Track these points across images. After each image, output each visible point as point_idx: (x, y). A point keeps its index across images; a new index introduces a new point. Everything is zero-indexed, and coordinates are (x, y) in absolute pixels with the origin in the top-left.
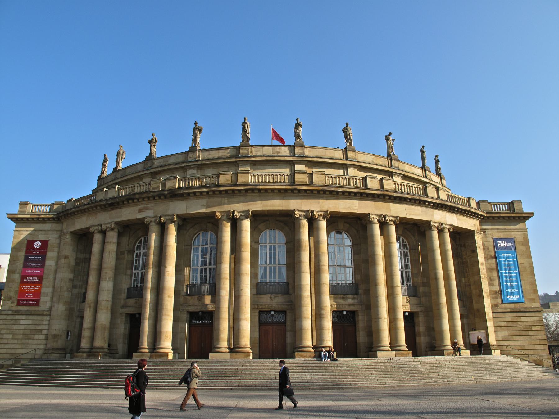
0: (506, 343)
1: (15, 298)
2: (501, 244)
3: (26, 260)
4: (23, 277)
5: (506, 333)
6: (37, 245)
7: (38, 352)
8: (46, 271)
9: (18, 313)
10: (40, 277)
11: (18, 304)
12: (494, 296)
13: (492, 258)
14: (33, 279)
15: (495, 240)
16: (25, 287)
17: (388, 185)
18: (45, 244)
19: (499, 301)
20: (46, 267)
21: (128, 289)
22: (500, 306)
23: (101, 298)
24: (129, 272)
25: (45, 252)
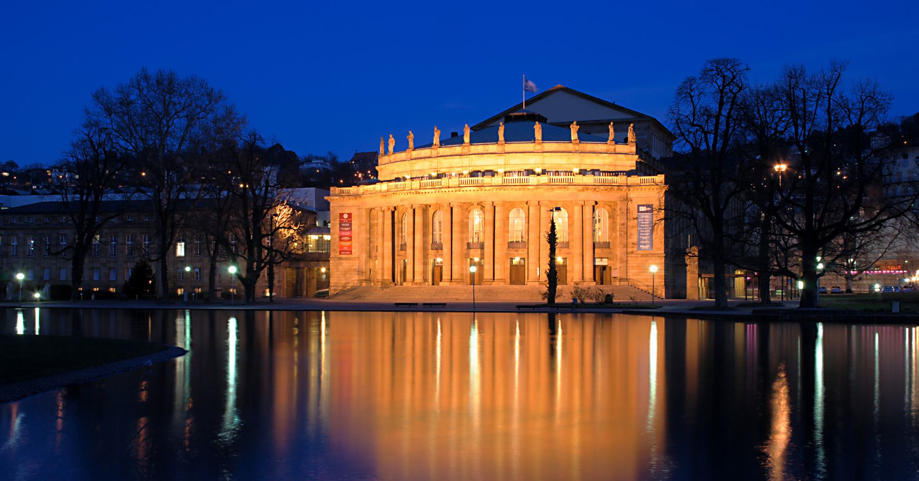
0: (634, 278)
1: (338, 250)
2: (643, 209)
3: (341, 226)
4: (341, 237)
5: (636, 271)
6: (346, 216)
7: (356, 282)
8: (353, 233)
9: (340, 259)
10: (350, 237)
11: (340, 254)
12: (631, 246)
13: (634, 219)
14: (347, 238)
15: (639, 206)
16: (343, 243)
17: (544, 180)
18: (350, 215)
19: (635, 249)
20: (353, 230)
21: (401, 245)
22: (634, 253)
23: (385, 252)
24: (400, 234)
25: (351, 221)
